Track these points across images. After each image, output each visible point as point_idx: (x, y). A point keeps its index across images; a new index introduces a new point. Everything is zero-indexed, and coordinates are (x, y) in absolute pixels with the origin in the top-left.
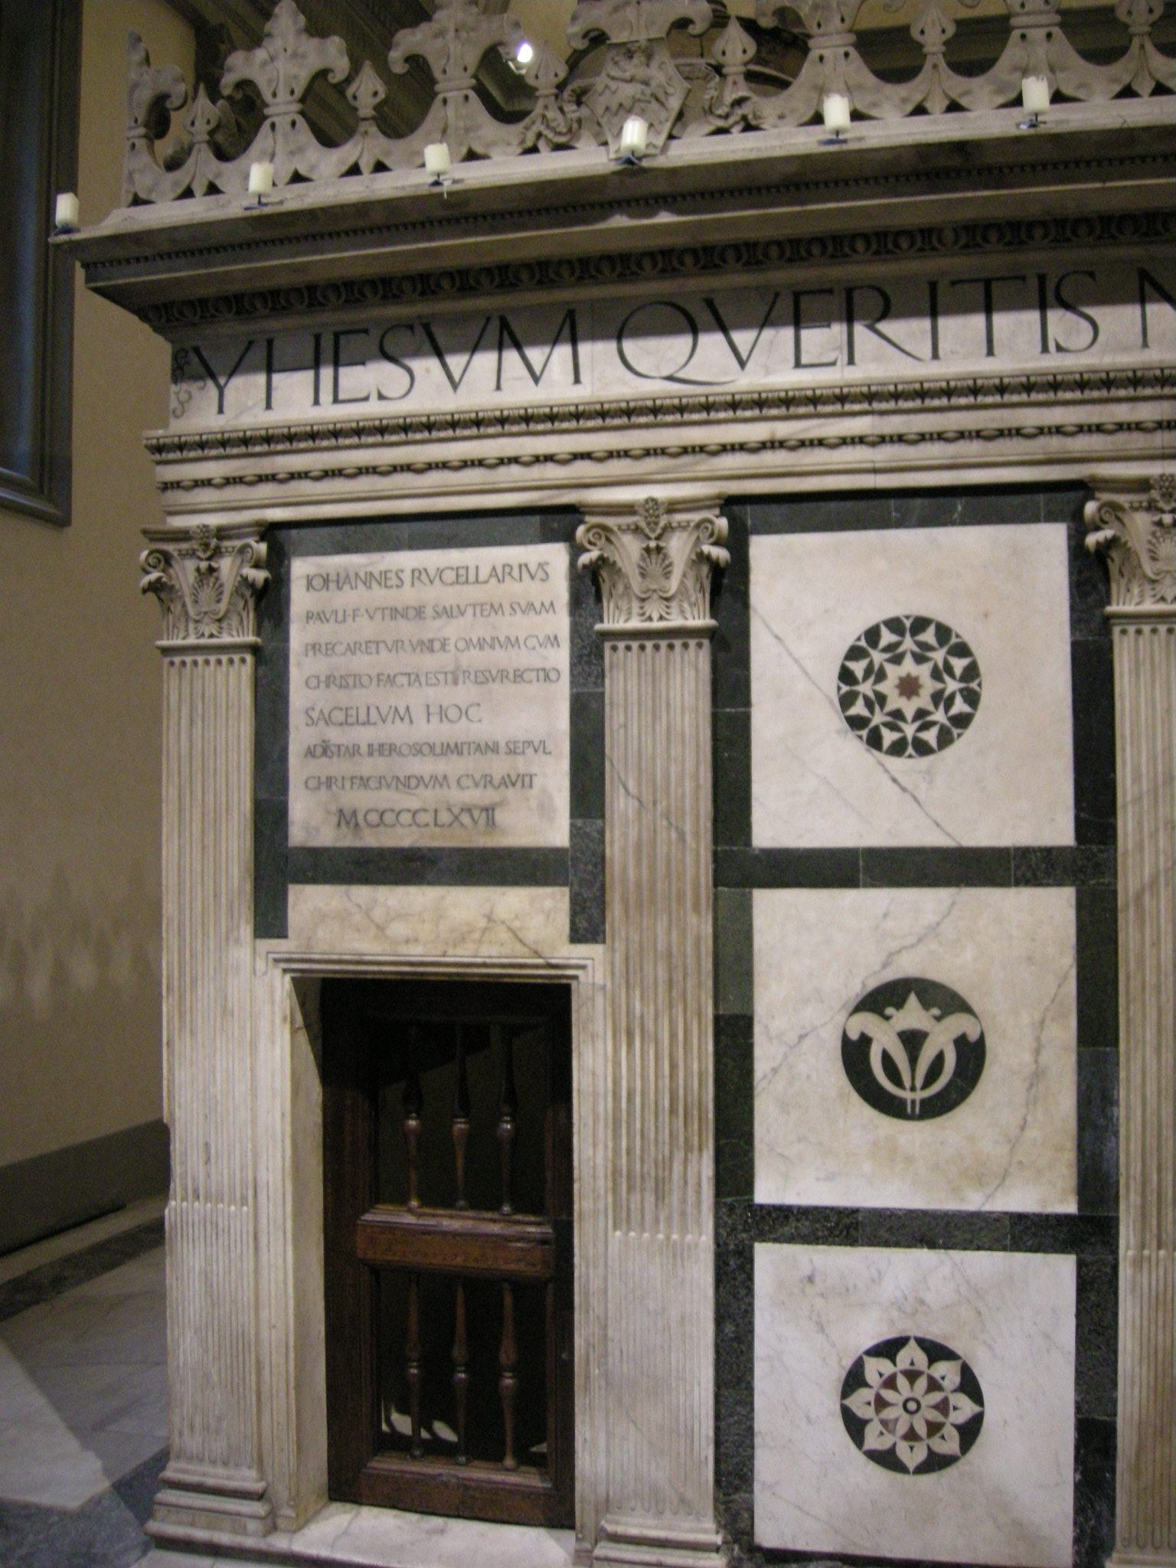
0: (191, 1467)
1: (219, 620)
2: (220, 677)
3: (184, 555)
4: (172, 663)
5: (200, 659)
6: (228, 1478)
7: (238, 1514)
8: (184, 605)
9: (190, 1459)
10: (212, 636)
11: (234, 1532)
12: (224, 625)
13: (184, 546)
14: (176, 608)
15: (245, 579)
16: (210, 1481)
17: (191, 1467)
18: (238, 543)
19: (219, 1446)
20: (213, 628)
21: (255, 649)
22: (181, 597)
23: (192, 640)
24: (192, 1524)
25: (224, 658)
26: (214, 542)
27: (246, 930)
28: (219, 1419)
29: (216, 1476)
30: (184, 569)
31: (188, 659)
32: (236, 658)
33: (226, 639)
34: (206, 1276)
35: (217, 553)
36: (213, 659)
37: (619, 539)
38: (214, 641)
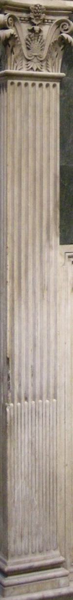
0: (21, 560)
1: (41, 61)
2: (39, 94)
3: (23, 20)
4: (12, 83)
5: (30, 83)
6: (45, 559)
7: (55, 577)
8: (21, 50)
9: (20, 556)
10: (37, 70)
11: (53, 588)
12: (44, 64)
13: (24, 15)
14: (16, 51)
15: (62, 38)
16: (36, 564)
17: (21, 560)
18: (58, 19)
19: (37, 542)
20: (38, 65)
21: (59, 79)
22: (21, 45)
23: (24, 71)
24: (28, 592)
25: (44, 83)
26: (43, 16)
27: (55, 239)
28: (38, 526)
29: (38, 560)
30: (21, 30)
31: (23, 82)
32: (51, 84)
33: (44, 72)
34: (32, 444)
35: (44, 22)
36: (37, 83)
37: (20, 26)
38: (38, 73)
